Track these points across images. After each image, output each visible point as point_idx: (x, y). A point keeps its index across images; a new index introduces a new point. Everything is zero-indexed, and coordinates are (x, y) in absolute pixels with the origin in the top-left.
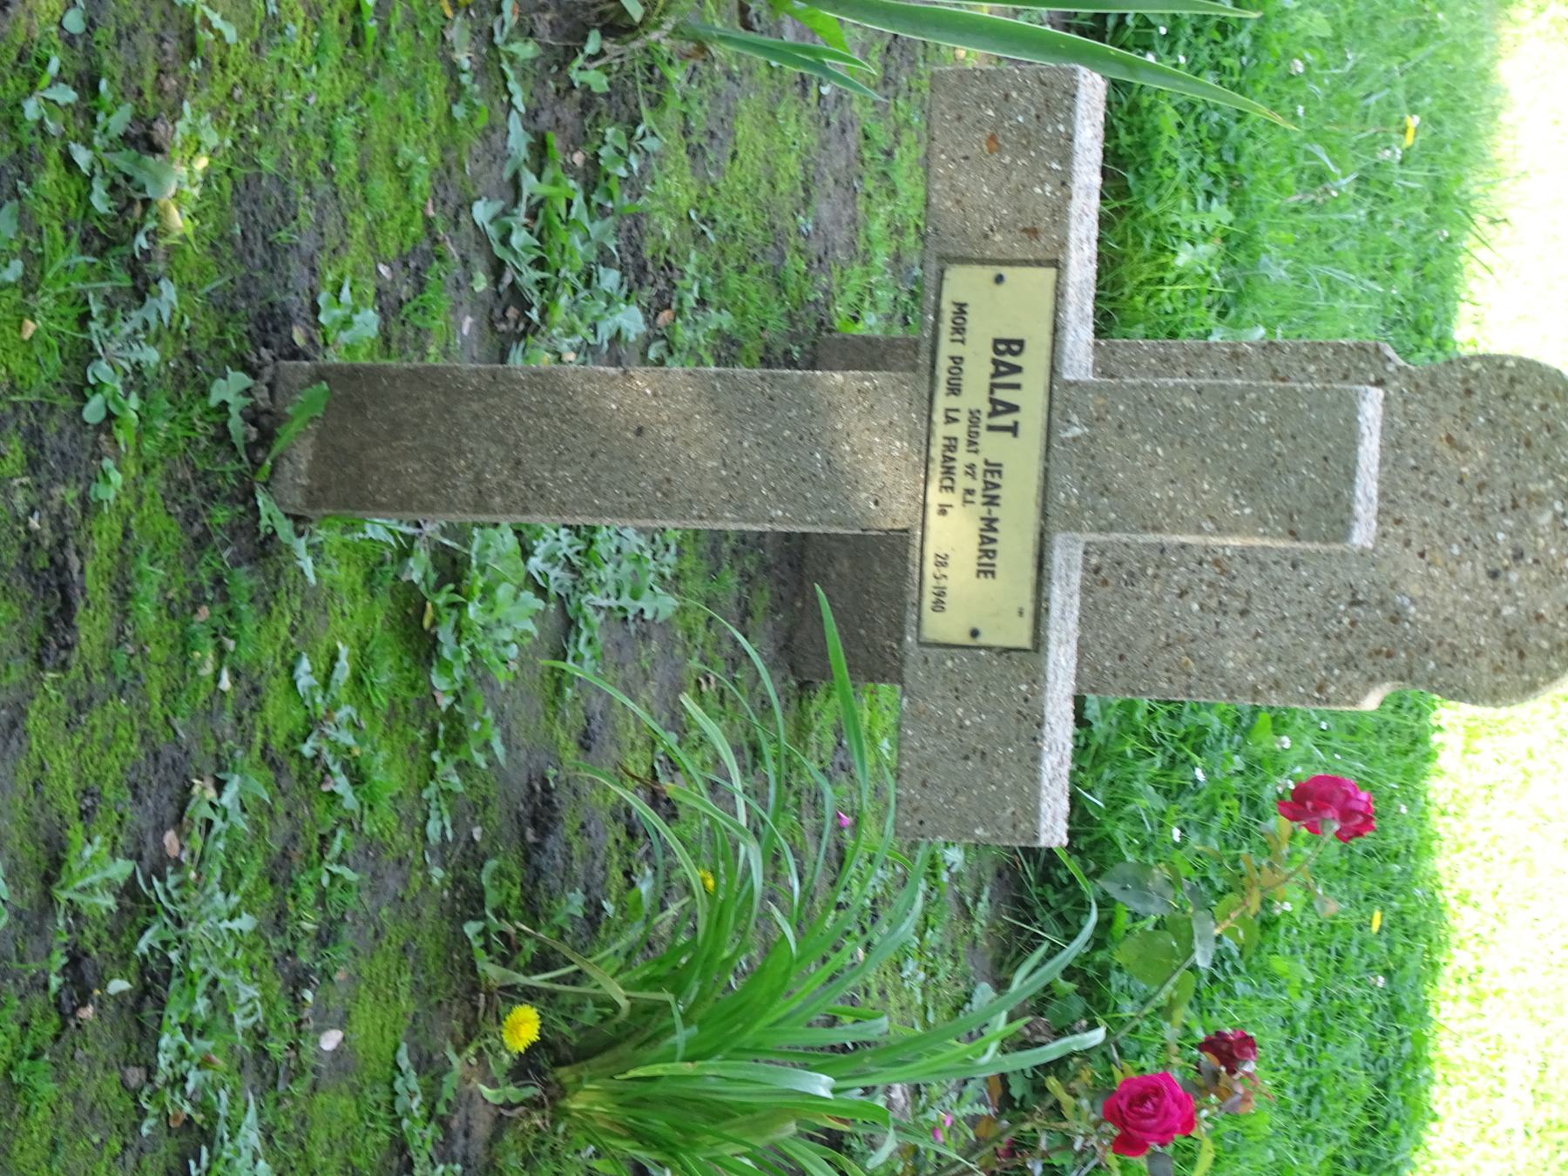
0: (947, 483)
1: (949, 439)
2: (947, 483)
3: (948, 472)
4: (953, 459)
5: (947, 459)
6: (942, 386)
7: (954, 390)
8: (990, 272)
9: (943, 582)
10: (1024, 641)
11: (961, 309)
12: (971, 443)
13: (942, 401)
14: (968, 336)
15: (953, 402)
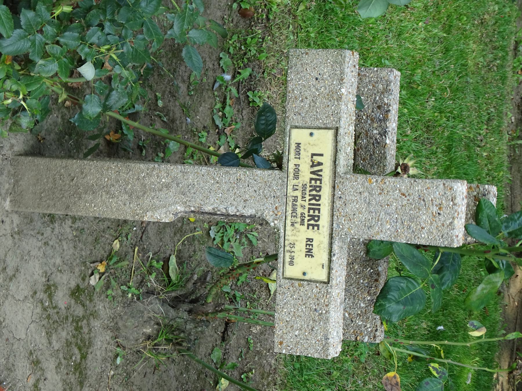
0: (294, 214)
1: (295, 197)
2: (294, 214)
3: (294, 210)
4: (296, 205)
5: (294, 205)
6: (291, 176)
7: (296, 176)
8: (310, 131)
9: (293, 254)
10: (324, 278)
11: (298, 145)
12: (303, 197)
13: (292, 182)
14: (301, 156)
15: (295, 182)
